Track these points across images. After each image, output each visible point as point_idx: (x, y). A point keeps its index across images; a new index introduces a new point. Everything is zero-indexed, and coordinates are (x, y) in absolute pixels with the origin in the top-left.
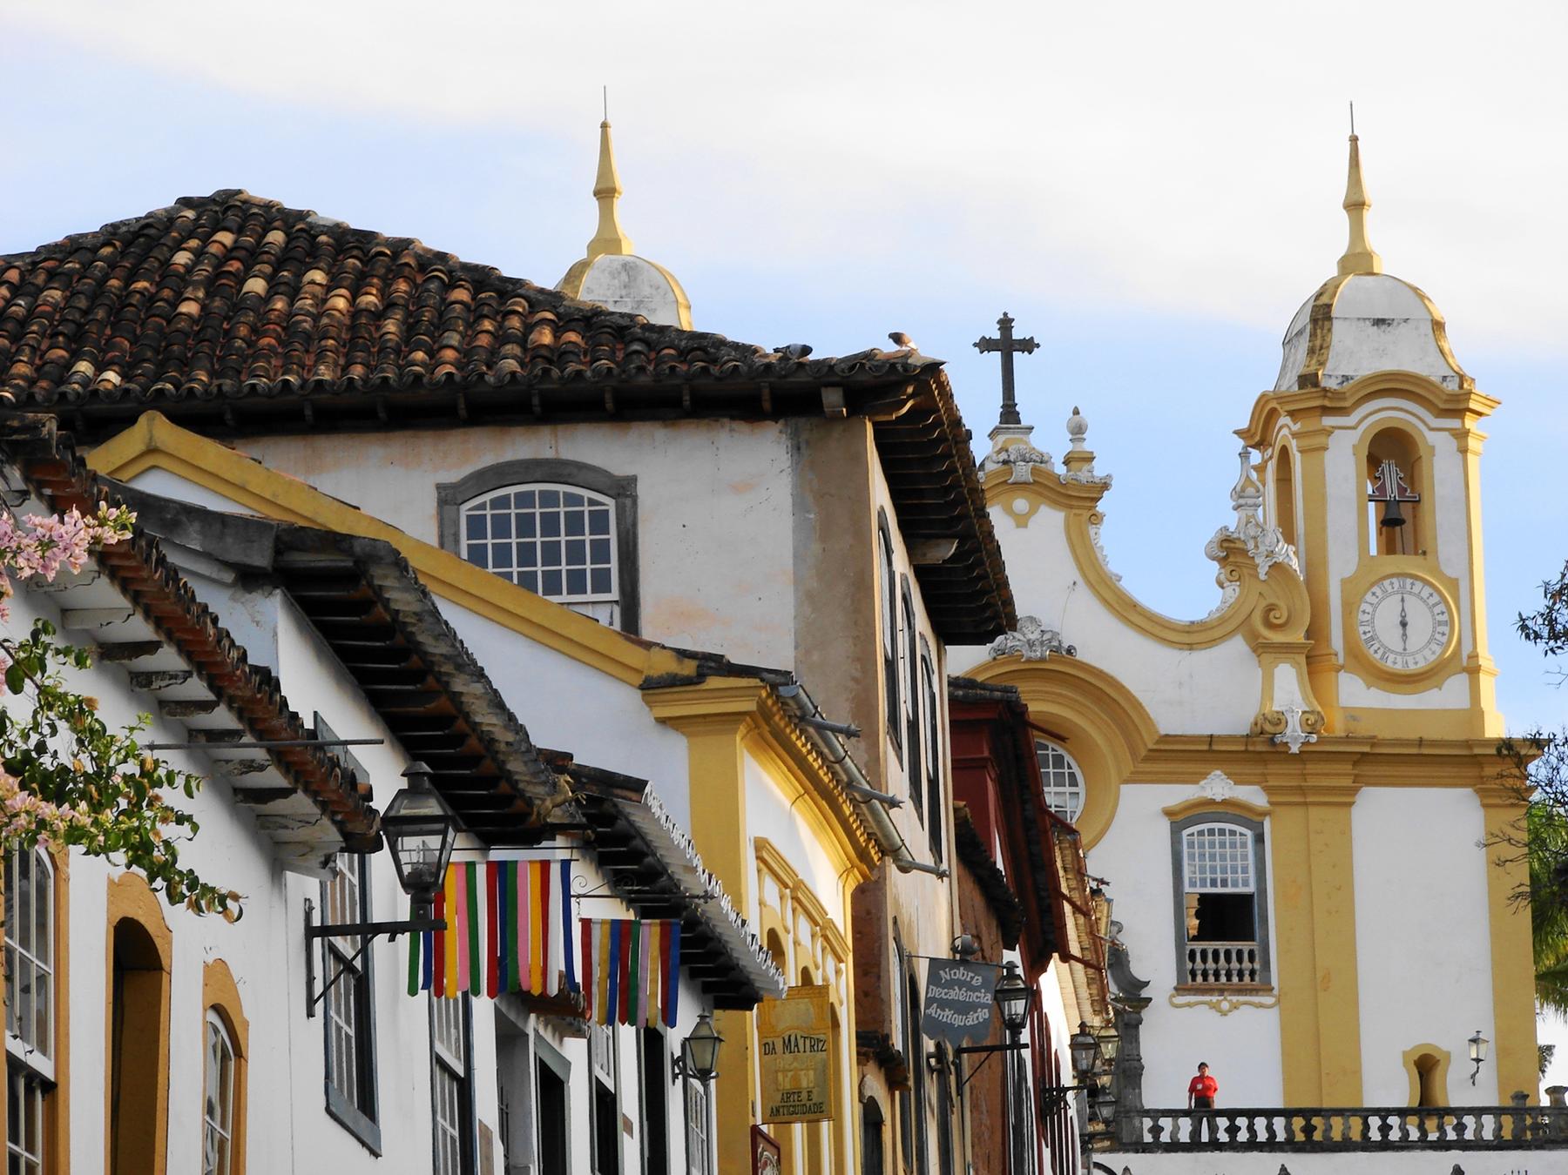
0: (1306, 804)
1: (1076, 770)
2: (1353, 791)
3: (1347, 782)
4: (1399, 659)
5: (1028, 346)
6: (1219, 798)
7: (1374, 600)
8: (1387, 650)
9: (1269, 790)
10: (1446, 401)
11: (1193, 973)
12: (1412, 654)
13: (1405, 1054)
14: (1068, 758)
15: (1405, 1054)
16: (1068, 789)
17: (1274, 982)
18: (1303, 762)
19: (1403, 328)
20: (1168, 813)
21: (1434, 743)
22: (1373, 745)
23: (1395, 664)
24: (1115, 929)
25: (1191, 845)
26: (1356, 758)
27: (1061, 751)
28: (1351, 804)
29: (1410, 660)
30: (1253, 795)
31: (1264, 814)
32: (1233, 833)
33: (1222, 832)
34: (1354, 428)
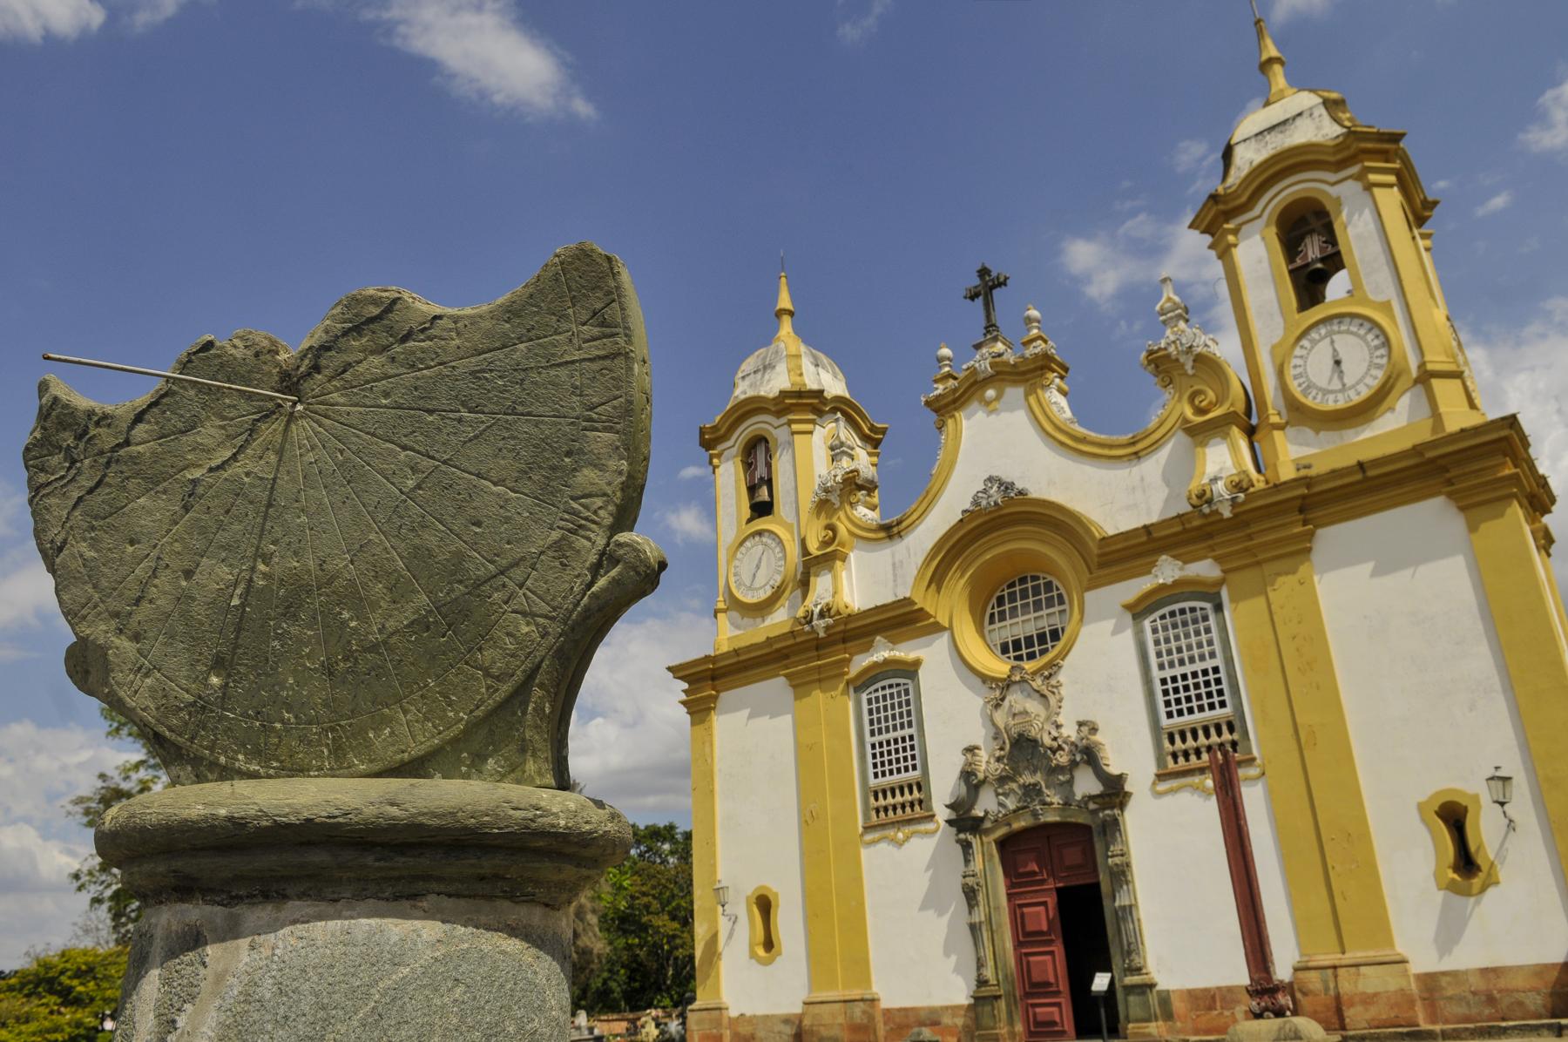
0: (1258, 563)
1: (1062, 591)
2: (1310, 535)
3: (1299, 529)
4: (1340, 396)
5: (1001, 283)
6: (1169, 581)
7: (1304, 352)
8: (1326, 392)
9: (1217, 559)
10: (1335, 154)
11: (1175, 756)
12: (1353, 386)
13: (1421, 807)
14: (1056, 582)
15: (1421, 807)
16: (1057, 609)
17: (1255, 753)
18: (1247, 524)
19: (1299, 121)
20: (1128, 607)
21: (1376, 463)
22: (1308, 487)
23: (1331, 404)
24: (1085, 729)
25: (1155, 631)
26: (1298, 503)
27: (1049, 578)
28: (1309, 550)
29: (1352, 393)
30: (1205, 569)
31: (1220, 583)
32: (1193, 610)
33: (1182, 612)
34: (1259, 217)
